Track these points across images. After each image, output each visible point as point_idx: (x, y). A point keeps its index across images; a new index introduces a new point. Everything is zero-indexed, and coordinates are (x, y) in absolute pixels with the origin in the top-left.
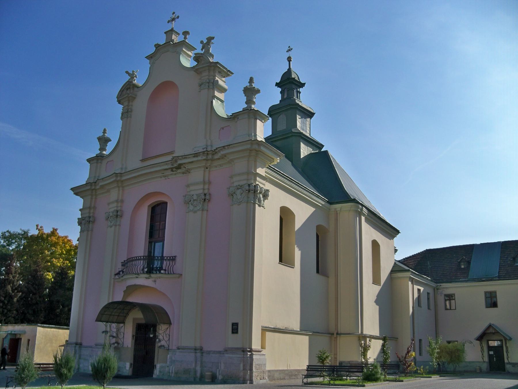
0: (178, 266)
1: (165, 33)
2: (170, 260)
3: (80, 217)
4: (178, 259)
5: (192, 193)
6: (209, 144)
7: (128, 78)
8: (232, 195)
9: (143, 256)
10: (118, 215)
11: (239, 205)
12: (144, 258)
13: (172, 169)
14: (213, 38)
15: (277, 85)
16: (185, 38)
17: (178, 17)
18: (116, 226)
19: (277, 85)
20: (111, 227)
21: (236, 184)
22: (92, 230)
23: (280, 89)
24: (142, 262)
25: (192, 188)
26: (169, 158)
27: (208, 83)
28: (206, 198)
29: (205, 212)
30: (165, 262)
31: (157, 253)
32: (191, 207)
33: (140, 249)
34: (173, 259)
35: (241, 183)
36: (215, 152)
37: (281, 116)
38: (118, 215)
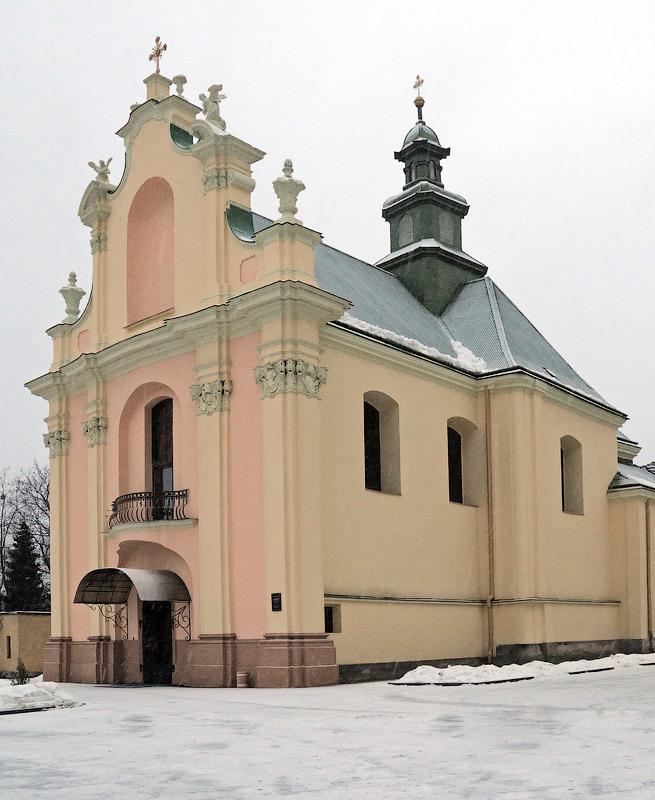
0: (191, 509)
1: (145, 81)
2: (179, 497)
3: (47, 432)
4: (191, 495)
5: (203, 381)
7: (93, 175)
8: (261, 379)
9: (145, 493)
10: (100, 426)
11: (272, 397)
12: (146, 496)
14: (220, 88)
15: (399, 156)
16: (180, 90)
17: (165, 47)
18: (99, 444)
19: (399, 156)
20: (92, 446)
21: (266, 361)
22: (67, 454)
23: (402, 165)
24: (135, 503)
25: (202, 373)
28: (225, 390)
29: (225, 413)
30: (177, 501)
31: (166, 488)
32: (203, 406)
33: (139, 482)
34: (184, 494)
35: (272, 360)
37: (404, 219)
38: (100, 426)
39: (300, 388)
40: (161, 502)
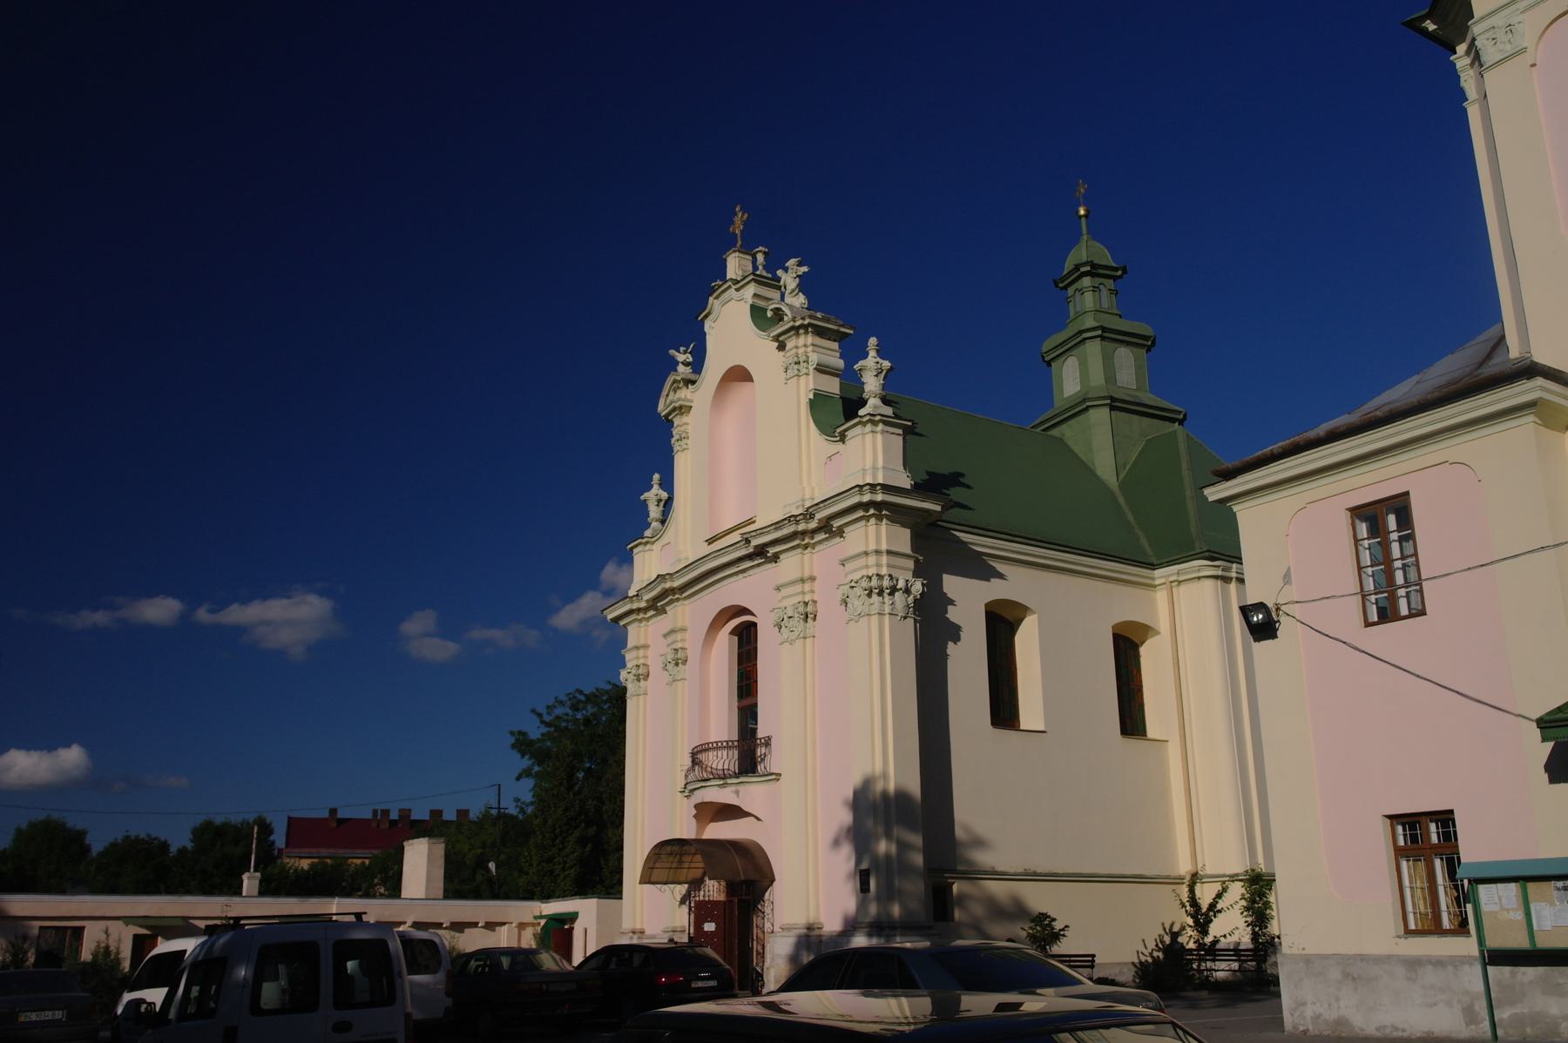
6: (807, 496)
13: (749, 557)
26: (735, 537)
27: (798, 363)
33: (722, 724)
36: (808, 515)
39: (887, 609)
40: (749, 753)
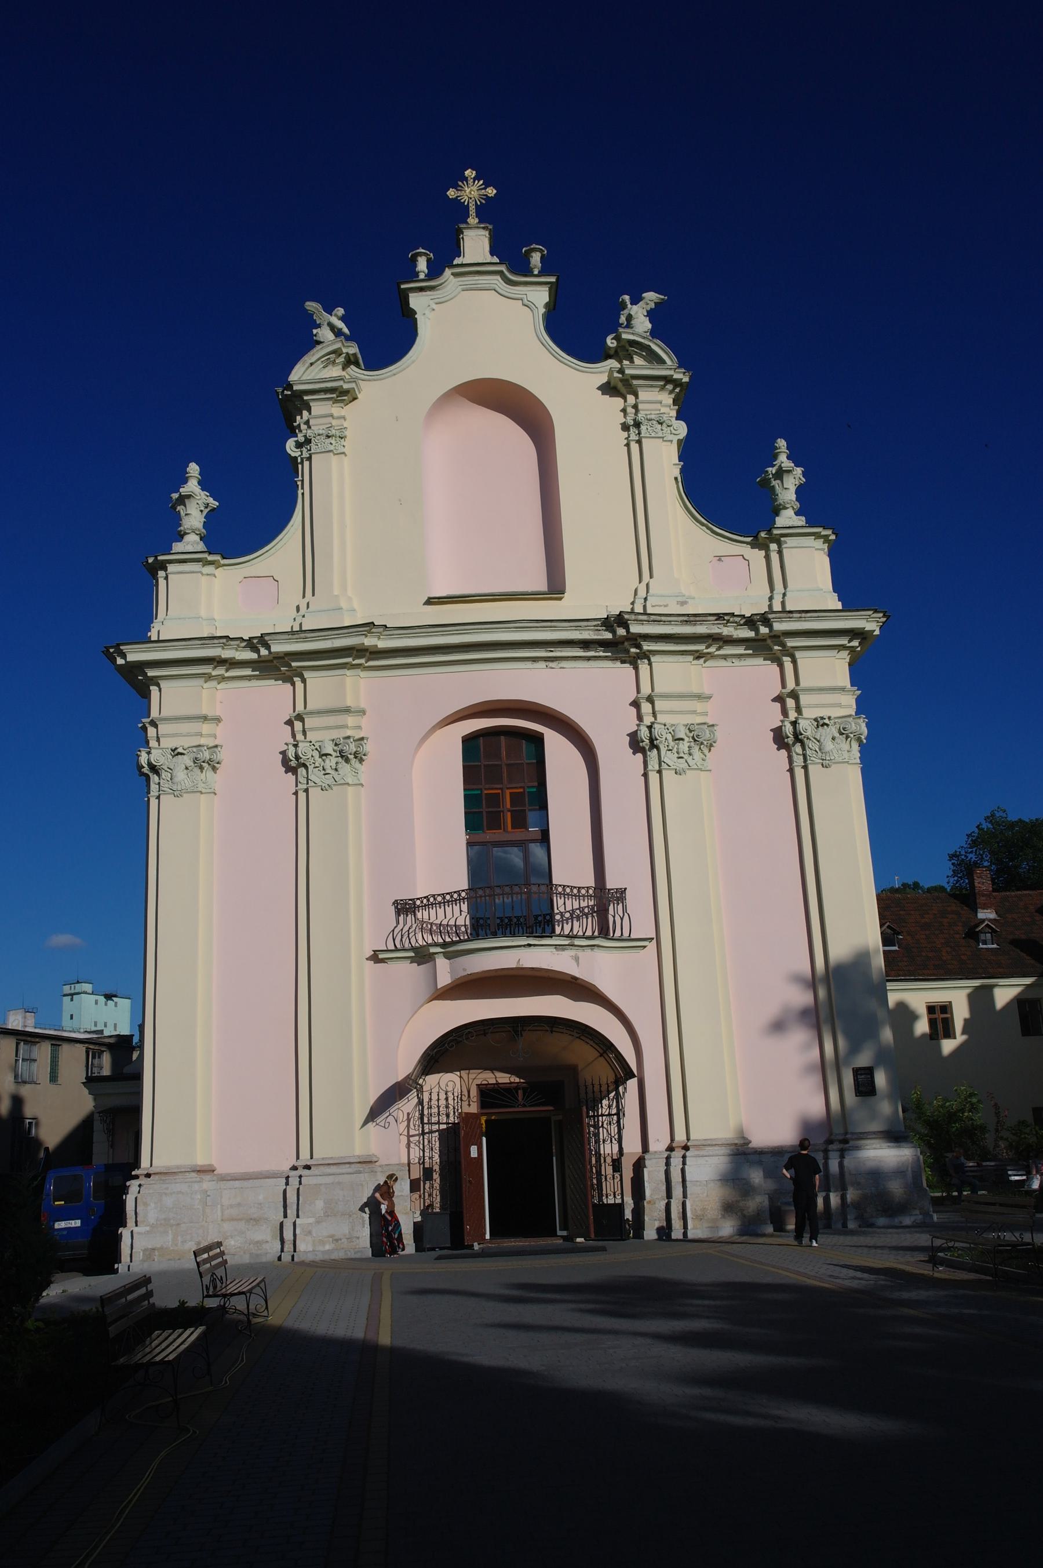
13: (585, 644)
